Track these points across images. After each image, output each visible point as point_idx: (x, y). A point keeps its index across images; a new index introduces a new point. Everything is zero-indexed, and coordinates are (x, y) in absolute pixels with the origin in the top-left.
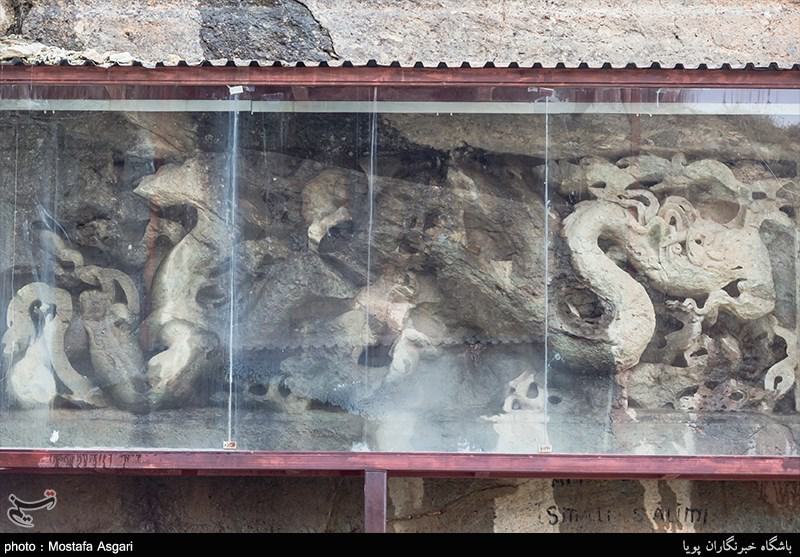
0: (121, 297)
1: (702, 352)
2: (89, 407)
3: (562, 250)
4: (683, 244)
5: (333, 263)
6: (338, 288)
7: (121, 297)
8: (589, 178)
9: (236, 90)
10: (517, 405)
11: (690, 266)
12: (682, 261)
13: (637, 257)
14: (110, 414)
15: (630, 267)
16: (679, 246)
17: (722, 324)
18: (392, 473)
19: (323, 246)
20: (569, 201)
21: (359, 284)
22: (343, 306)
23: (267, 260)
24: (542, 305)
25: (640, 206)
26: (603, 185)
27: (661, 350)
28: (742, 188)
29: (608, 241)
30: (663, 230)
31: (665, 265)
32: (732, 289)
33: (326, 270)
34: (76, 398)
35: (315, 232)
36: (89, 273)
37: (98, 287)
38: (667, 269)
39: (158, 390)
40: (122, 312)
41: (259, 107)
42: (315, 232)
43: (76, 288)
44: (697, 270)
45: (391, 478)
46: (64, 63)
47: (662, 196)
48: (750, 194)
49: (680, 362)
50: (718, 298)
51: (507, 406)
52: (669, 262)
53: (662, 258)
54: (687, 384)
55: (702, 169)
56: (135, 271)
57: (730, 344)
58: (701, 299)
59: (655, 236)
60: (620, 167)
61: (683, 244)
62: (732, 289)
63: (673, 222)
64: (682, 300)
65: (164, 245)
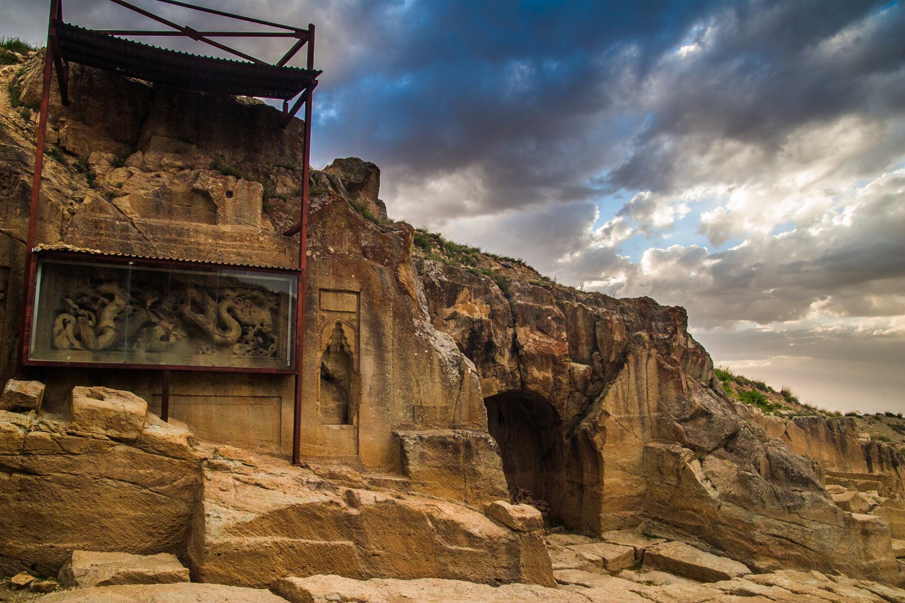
1: (253, 341)
2: (80, 350)
4: (250, 312)
5: (152, 312)
6: (155, 320)
7: (90, 319)
9: (131, 263)
10: (203, 353)
12: (249, 317)
14: (86, 352)
15: (235, 317)
17: (259, 333)
18: (171, 371)
19: (150, 307)
20: (220, 299)
22: (155, 324)
23: (134, 311)
24: (211, 327)
25: (239, 302)
26: (228, 295)
27: (241, 339)
29: (230, 310)
32: (262, 325)
33: (151, 314)
34: (76, 347)
35: (149, 303)
36: (82, 312)
37: (84, 316)
38: (246, 319)
39: (101, 346)
40: (91, 323)
41: (135, 268)
42: (149, 303)
43: (77, 316)
46: (80, 251)
47: (244, 299)
49: (247, 343)
50: (258, 326)
51: (201, 352)
54: (249, 349)
55: (255, 293)
56: (94, 312)
57: (261, 340)
58: (254, 327)
59: (242, 310)
61: (250, 312)
62: (262, 325)
63: (247, 306)
64: (248, 327)
65: (104, 305)
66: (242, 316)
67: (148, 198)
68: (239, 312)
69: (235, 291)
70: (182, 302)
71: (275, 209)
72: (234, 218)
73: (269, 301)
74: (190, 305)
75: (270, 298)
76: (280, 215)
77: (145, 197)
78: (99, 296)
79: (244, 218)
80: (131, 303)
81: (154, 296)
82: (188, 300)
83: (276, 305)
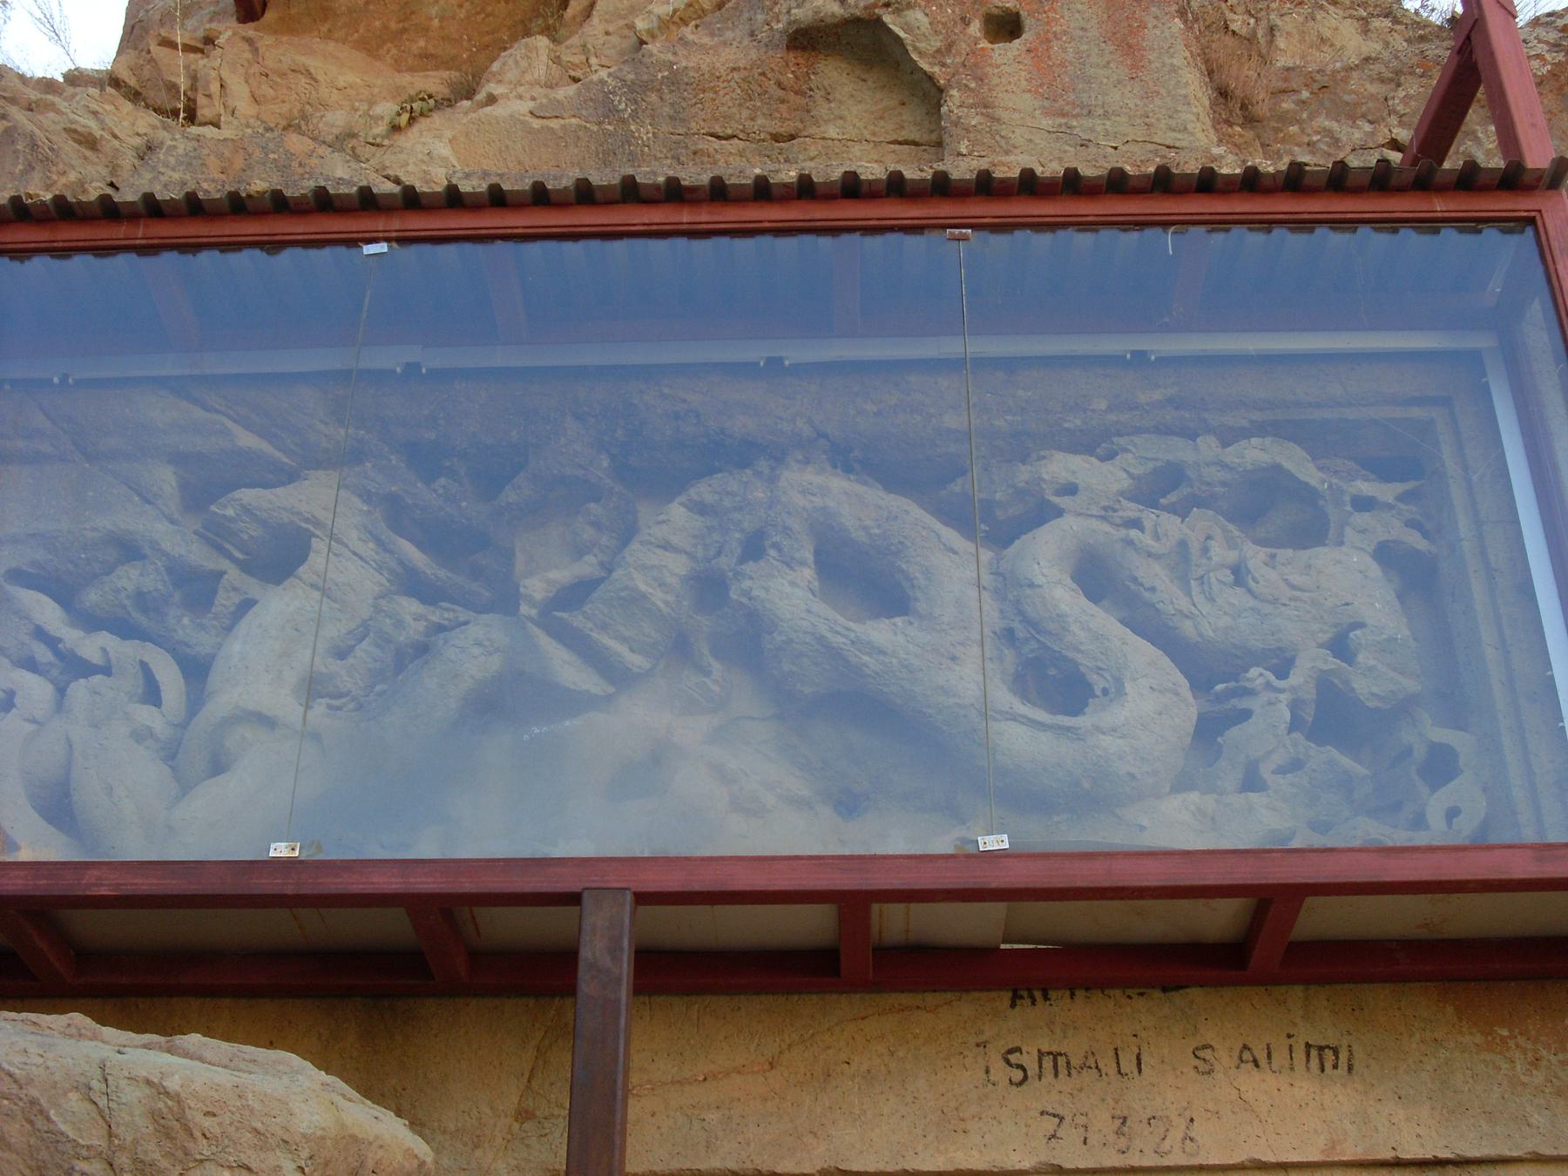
0: (152, 694)
3: (1009, 587)
8: (1046, 477)
11: (1252, 603)
12: (1237, 597)
13: (1147, 595)
16: (1228, 572)
21: (618, 677)
26: (1071, 490)
28: (1330, 486)
30: (1195, 546)
31: (1205, 608)
32: (1340, 647)
35: (536, 587)
44: (1268, 609)
45: (641, 908)
48: (1347, 498)
49: (1252, 782)
52: (1212, 600)
53: (1198, 598)
55: (1254, 453)
60: (1102, 459)
62: (1340, 647)
66: (1183, 603)
67: (554, 124)
68: (1156, 578)
69: (1109, 456)
70: (754, 549)
71: (1287, 105)
72: (1046, 123)
73: (1364, 504)
74: (808, 573)
75: (1366, 488)
76: (1328, 132)
77: (536, 124)
78: (225, 564)
79: (1106, 115)
80: (412, 584)
81: (579, 552)
82: (787, 531)
83: (1411, 524)
